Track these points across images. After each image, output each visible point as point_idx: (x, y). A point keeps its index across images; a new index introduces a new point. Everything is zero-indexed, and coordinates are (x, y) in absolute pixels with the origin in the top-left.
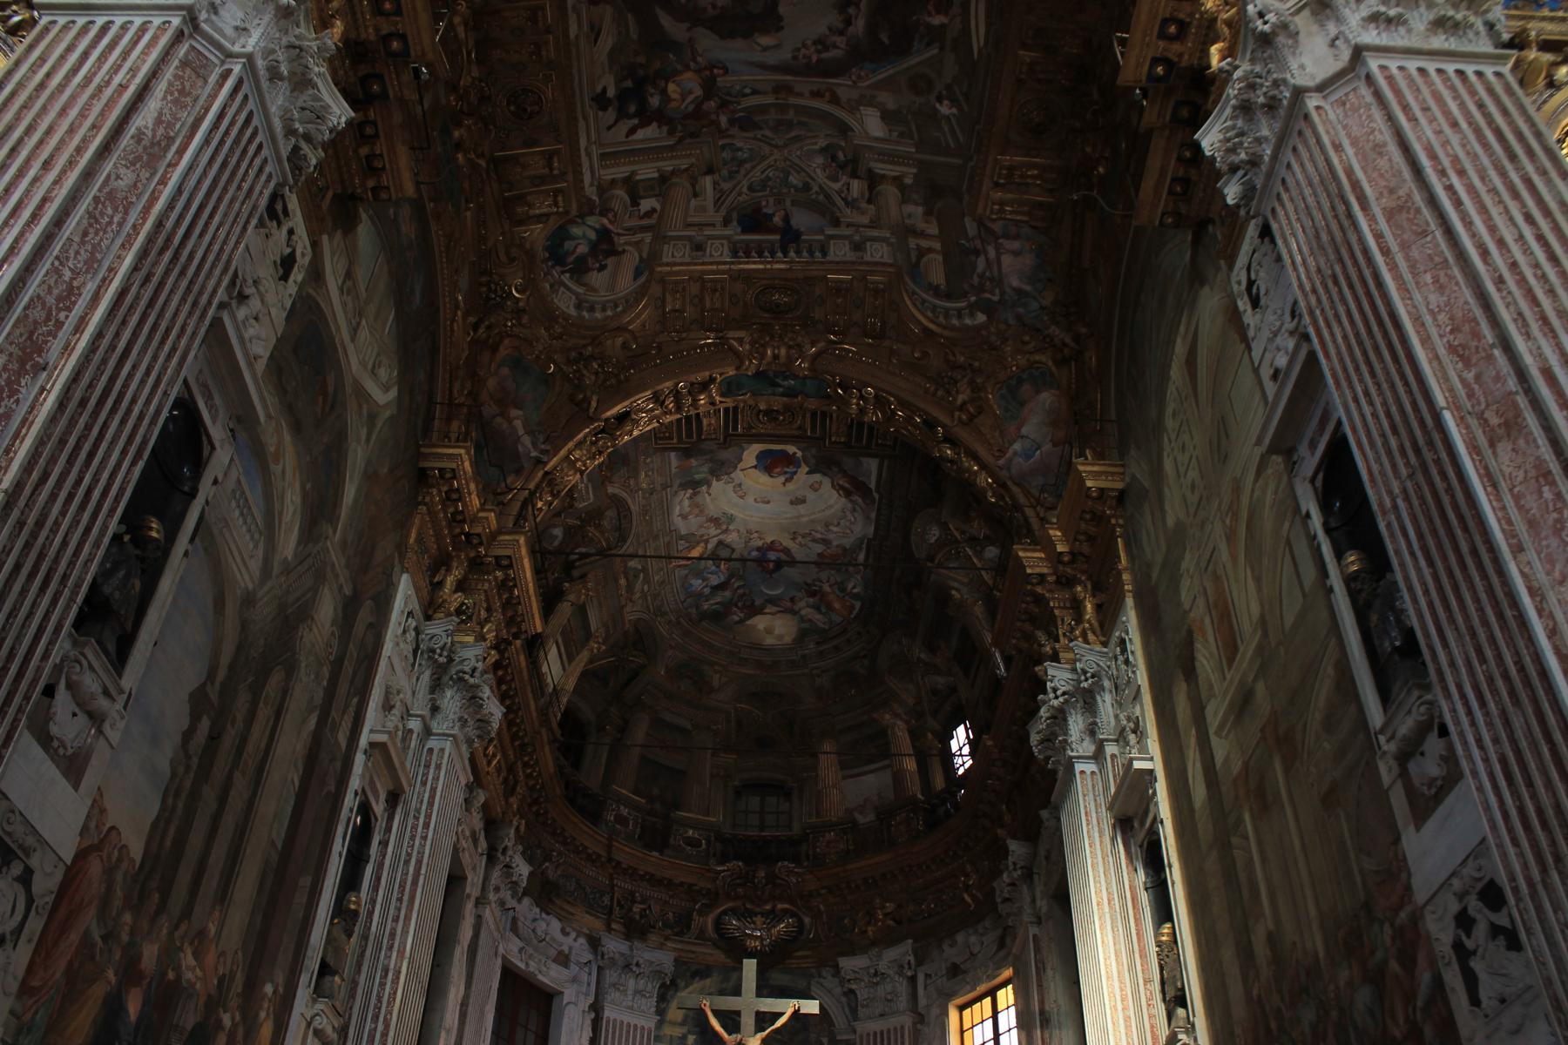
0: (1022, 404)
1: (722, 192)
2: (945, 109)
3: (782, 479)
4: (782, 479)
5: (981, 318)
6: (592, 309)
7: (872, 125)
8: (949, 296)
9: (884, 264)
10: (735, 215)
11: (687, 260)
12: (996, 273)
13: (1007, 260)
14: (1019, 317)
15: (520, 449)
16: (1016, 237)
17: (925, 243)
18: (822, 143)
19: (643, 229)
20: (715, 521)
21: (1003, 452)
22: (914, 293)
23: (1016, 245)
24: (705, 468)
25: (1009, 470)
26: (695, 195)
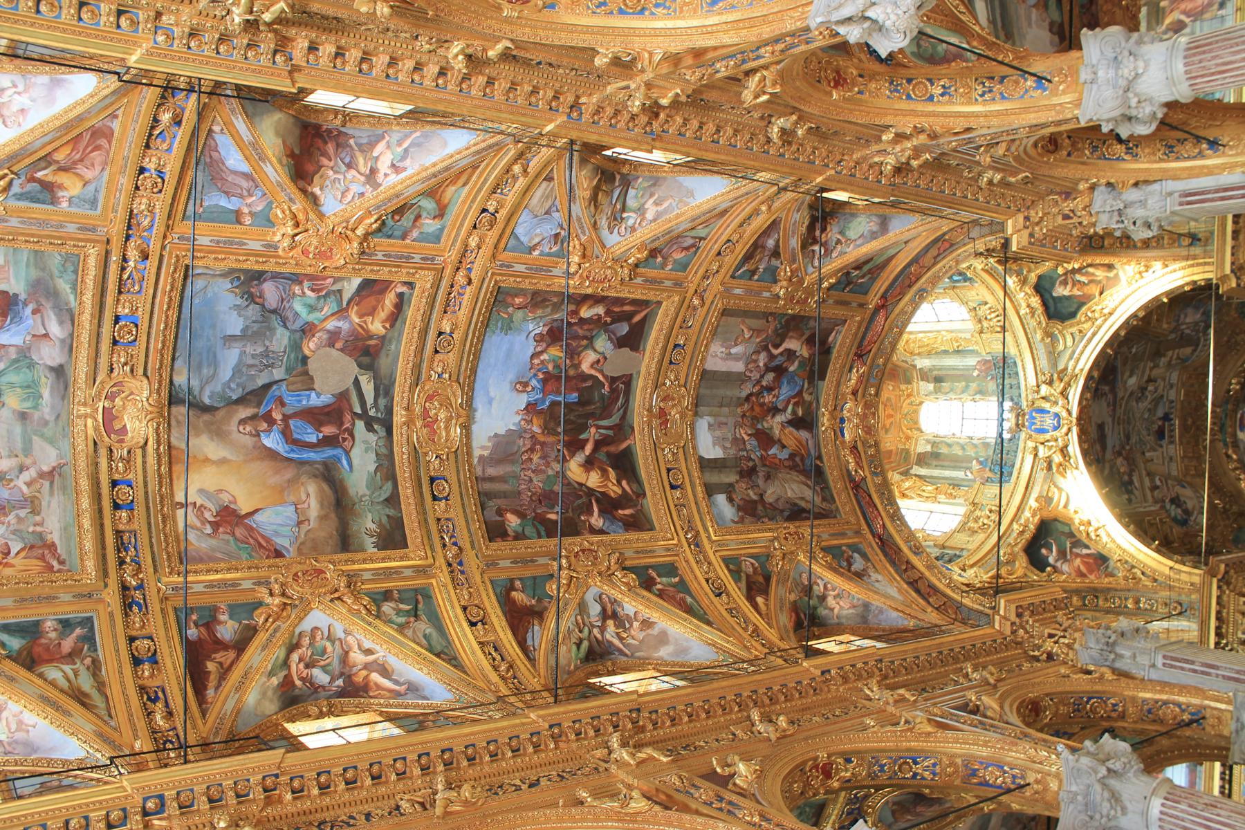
7: (1132, 381)
13: (1188, 320)
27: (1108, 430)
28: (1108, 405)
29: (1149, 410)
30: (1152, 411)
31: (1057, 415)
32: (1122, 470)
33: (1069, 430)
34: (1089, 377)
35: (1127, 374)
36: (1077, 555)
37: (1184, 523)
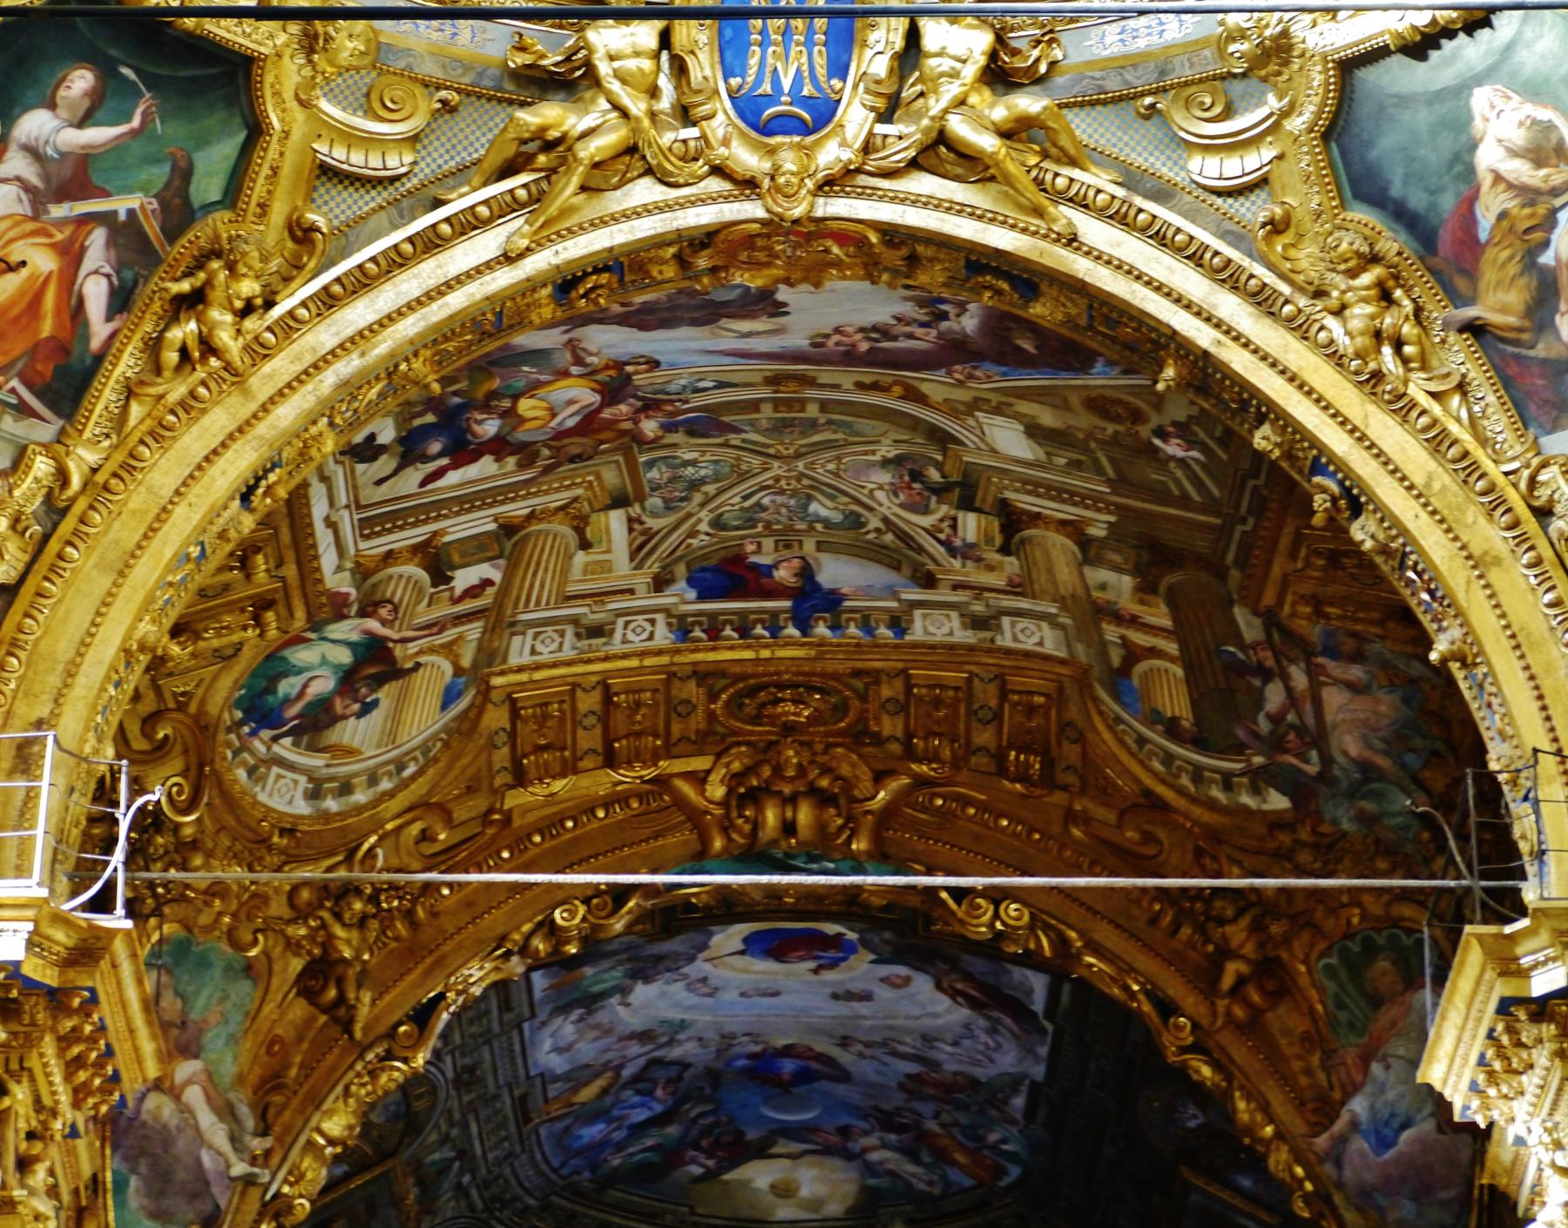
0: (1376, 1002)
1: (649, 534)
2: (1173, 448)
3: (812, 964)
4: (812, 964)
5: (1278, 801)
6: (346, 789)
8: (1199, 744)
9: (1046, 658)
10: (681, 570)
11: (568, 653)
12: (1310, 721)
13: (1334, 699)
14: (1364, 819)
15: (206, 1159)
16: (1357, 657)
17: (1139, 638)
18: (887, 450)
19: (459, 619)
20: (644, 1036)
21: (1324, 1109)
22: (1118, 720)
23: (1356, 672)
24: (618, 973)
25: (1339, 1164)
26: (585, 545)
27: (735, 333)
28: (883, 331)
29: (854, 522)
30: (850, 535)
31: (822, 115)
32: (525, 406)
33: (748, 185)
34: (1026, 278)
35: (1047, 418)
36: (71, 255)
37: (260, 710)
